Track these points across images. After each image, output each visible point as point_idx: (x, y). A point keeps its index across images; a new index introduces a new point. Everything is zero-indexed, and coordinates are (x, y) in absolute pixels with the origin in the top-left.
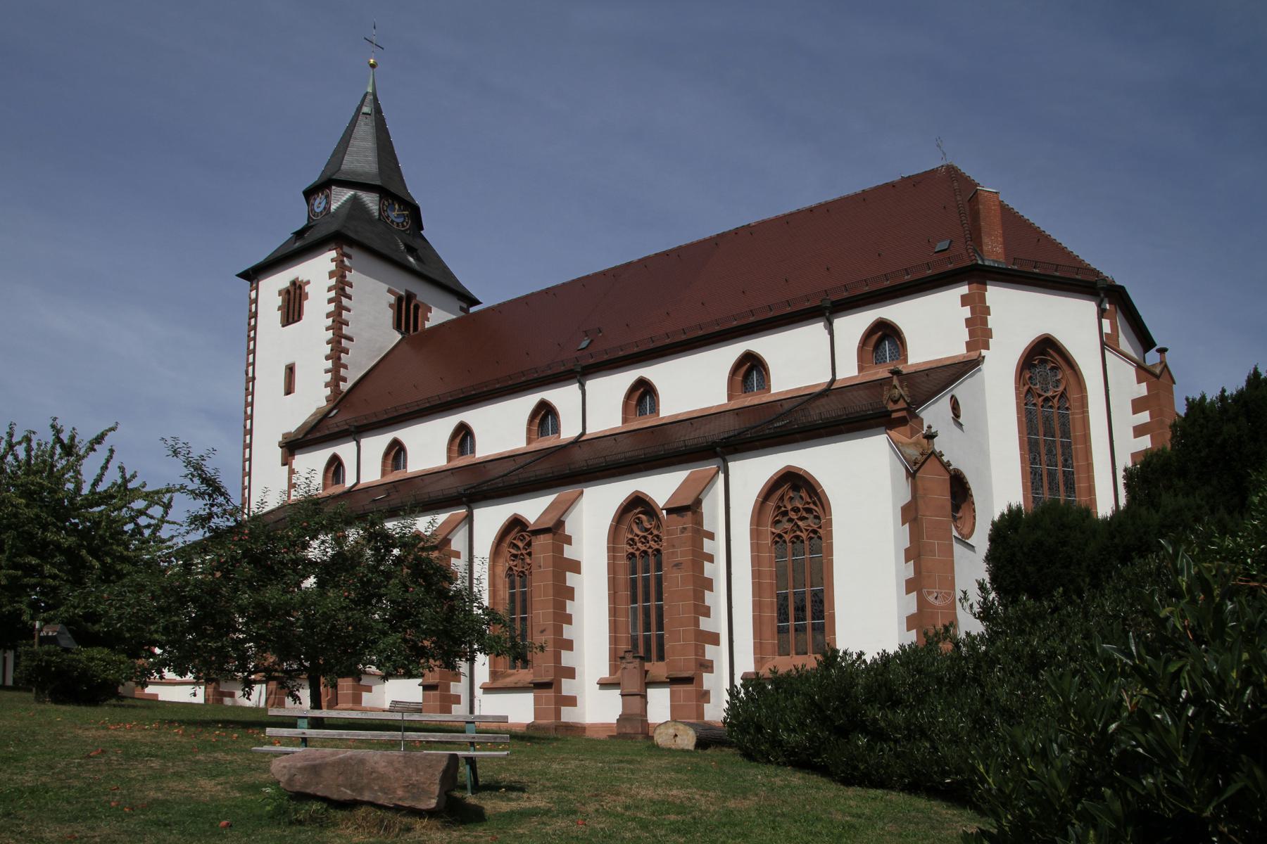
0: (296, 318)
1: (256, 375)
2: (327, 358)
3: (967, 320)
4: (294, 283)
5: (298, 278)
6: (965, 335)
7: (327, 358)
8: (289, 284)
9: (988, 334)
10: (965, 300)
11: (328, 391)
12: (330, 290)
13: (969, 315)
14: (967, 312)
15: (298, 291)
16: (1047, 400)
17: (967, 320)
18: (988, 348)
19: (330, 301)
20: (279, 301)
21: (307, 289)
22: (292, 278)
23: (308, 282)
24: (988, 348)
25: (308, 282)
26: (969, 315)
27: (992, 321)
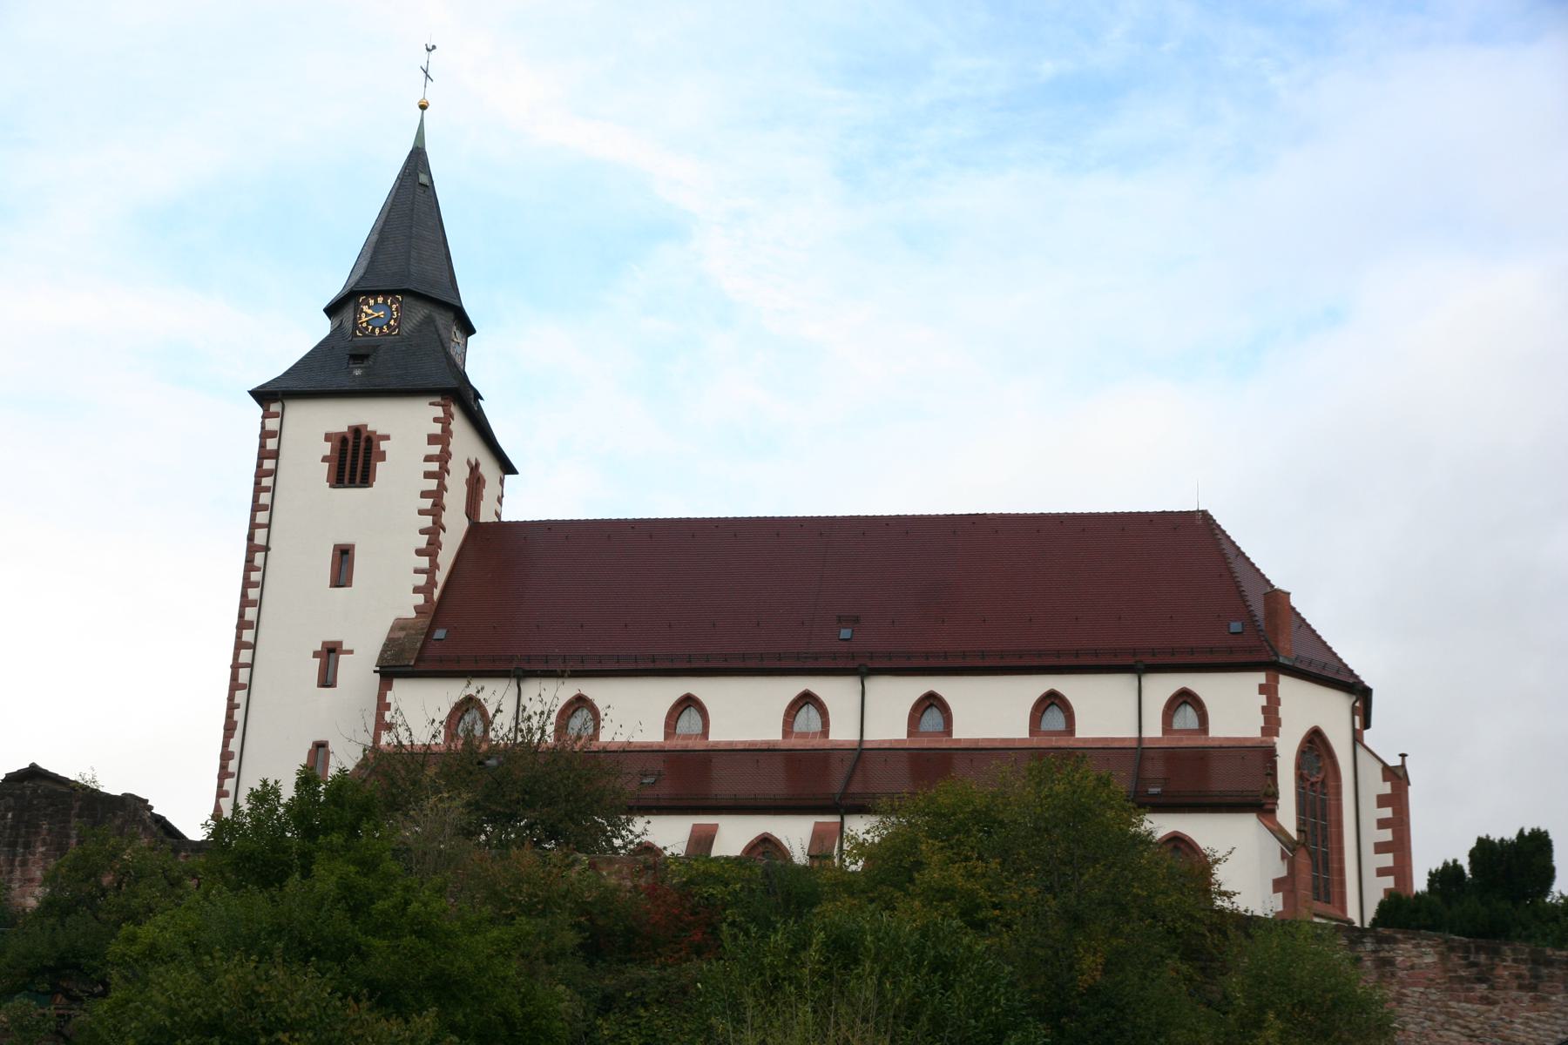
0: (358, 479)
1: (271, 545)
2: (419, 552)
3: (1263, 708)
4: (357, 431)
5: (366, 426)
6: (1260, 721)
7: (419, 552)
8: (346, 430)
9: (1278, 722)
10: (1263, 689)
11: (420, 599)
12: (428, 459)
13: (1265, 704)
14: (1263, 700)
15: (362, 444)
16: (1312, 784)
17: (1263, 708)
18: (1277, 735)
19: (428, 475)
20: (326, 449)
21: (383, 445)
22: (355, 422)
23: (387, 438)
24: (1277, 735)
25: (387, 438)
26: (1265, 704)
27: (1283, 711)
